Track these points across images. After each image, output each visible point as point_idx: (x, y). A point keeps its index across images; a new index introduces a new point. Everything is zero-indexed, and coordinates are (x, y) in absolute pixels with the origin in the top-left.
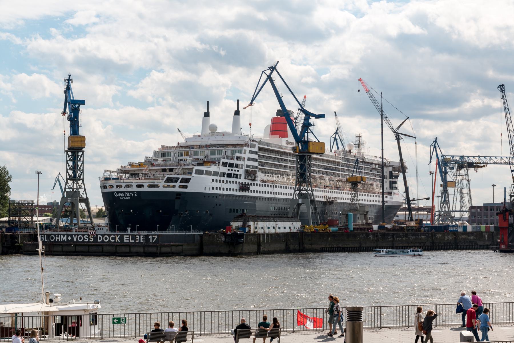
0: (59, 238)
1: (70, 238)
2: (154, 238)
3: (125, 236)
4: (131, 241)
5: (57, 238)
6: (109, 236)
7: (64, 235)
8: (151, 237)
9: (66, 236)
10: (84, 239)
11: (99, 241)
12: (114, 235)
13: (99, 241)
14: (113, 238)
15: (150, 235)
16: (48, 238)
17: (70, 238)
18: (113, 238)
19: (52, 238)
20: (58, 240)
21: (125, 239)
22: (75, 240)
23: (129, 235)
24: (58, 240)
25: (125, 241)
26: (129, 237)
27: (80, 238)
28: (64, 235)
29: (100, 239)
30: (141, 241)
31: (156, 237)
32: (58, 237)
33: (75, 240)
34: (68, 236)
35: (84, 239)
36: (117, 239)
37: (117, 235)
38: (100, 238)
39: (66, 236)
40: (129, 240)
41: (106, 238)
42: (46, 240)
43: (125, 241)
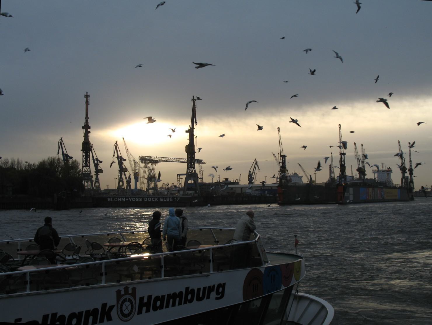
0: (120, 200)
1: (127, 199)
2: (178, 199)
3: (161, 198)
4: (164, 200)
5: (119, 199)
6: (151, 198)
7: (123, 198)
8: (175, 198)
9: (124, 199)
10: (136, 200)
11: (145, 200)
12: (155, 198)
13: (145, 200)
14: (153, 199)
15: (175, 198)
16: (113, 199)
17: (127, 199)
18: (153, 199)
19: (116, 199)
20: (120, 200)
21: (161, 199)
22: (130, 200)
23: (163, 198)
24: (120, 200)
25: (161, 200)
26: (163, 199)
27: (134, 199)
28: (123, 198)
29: (146, 199)
30: (170, 200)
31: (179, 198)
32: (120, 199)
33: (130, 200)
34: (126, 198)
35: (136, 200)
36: (156, 200)
37: (157, 198)
38: (146, 199)
39: (124, 199)
40: (163, 200)
41: (149, 199)
42: (112, 201)
43: (161, 200)
